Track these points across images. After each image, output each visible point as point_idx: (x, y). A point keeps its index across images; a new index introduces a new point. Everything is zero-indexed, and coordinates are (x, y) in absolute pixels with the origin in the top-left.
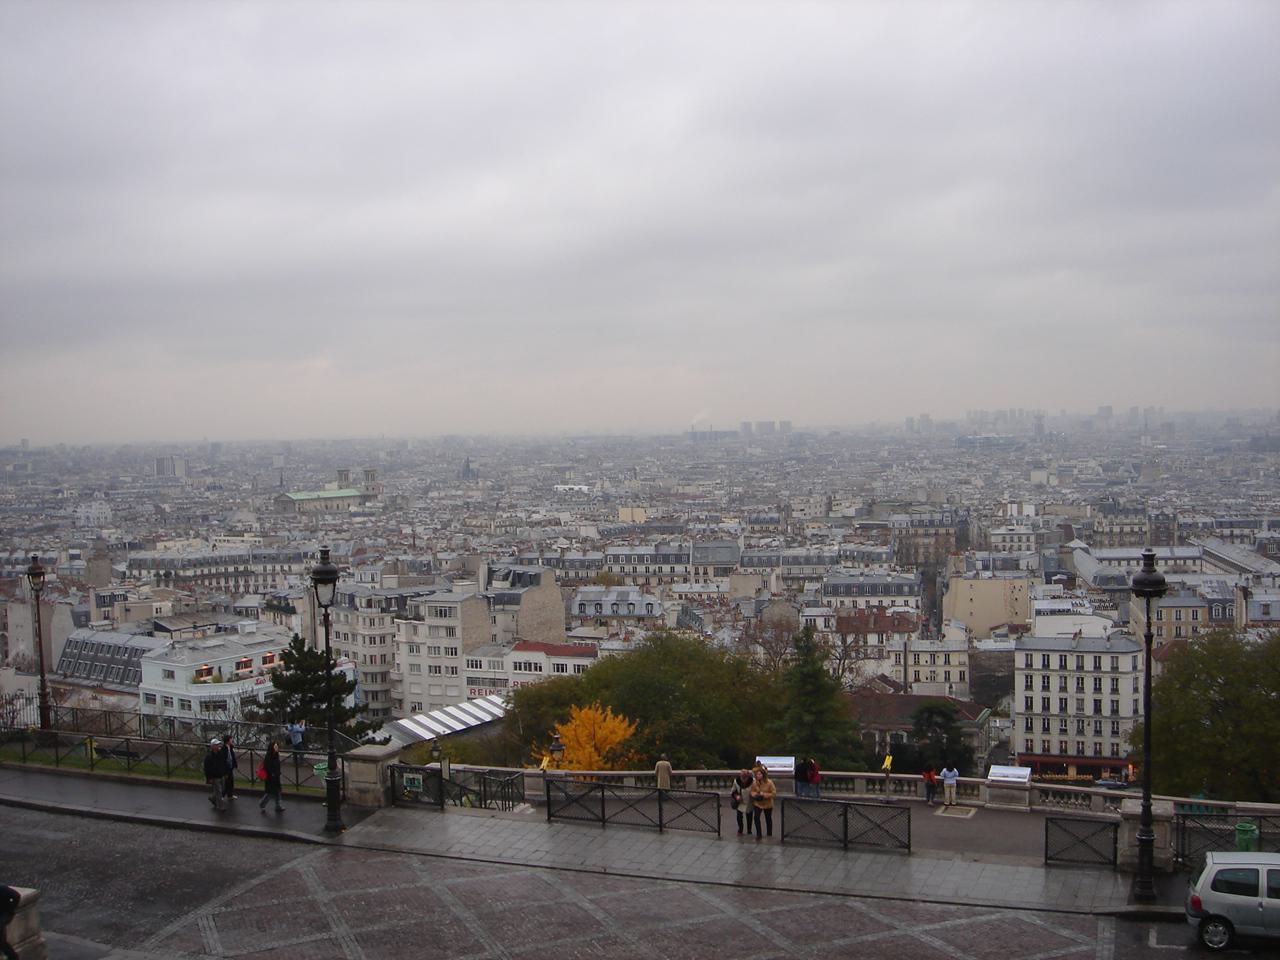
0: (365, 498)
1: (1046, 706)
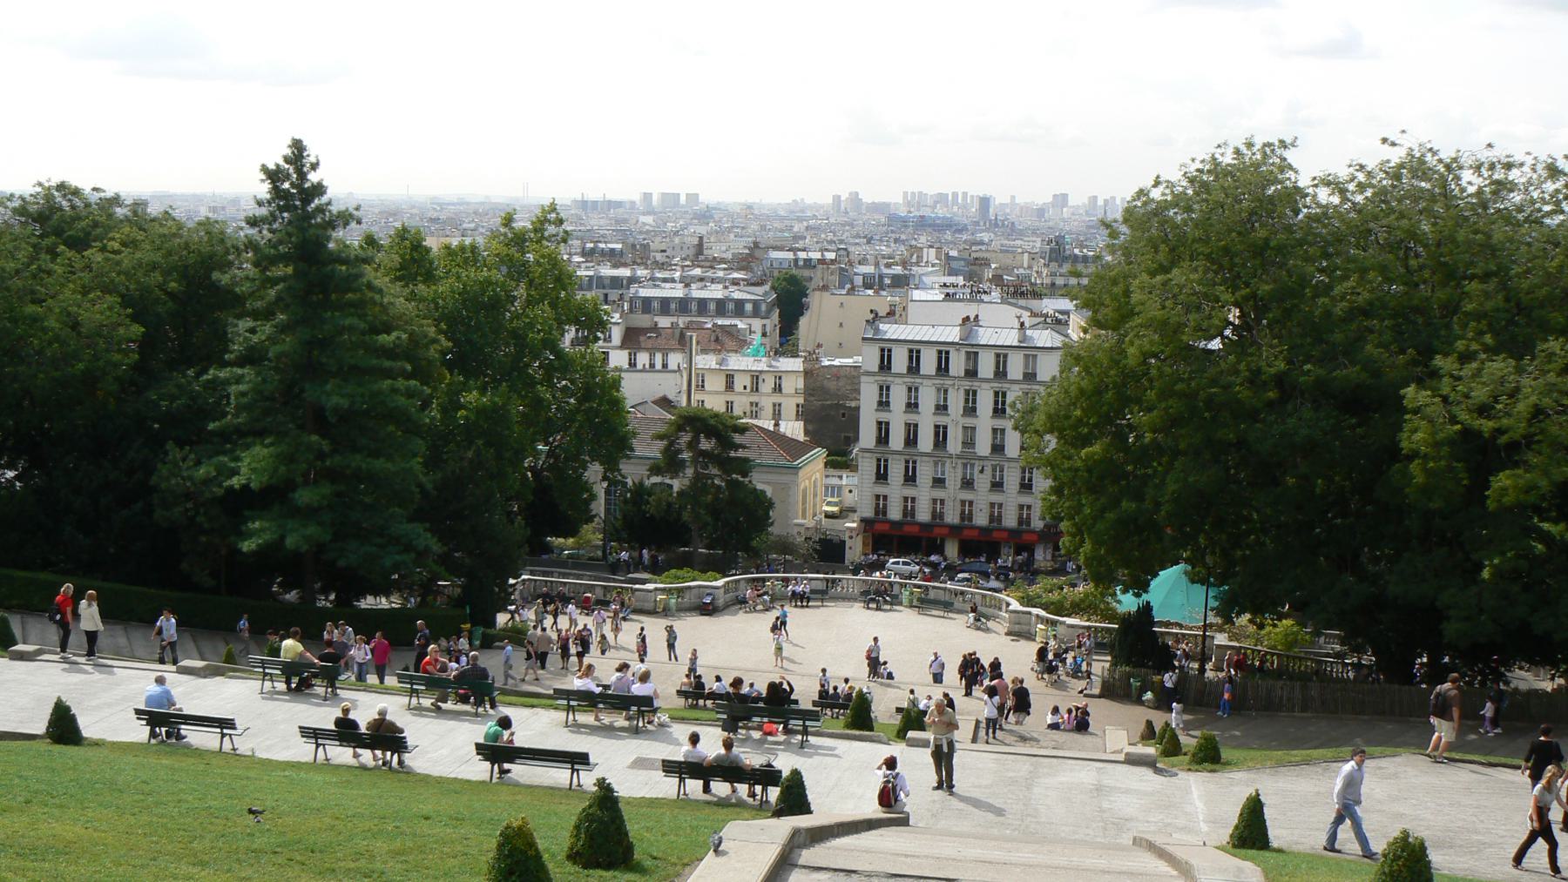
1: (911, 439)
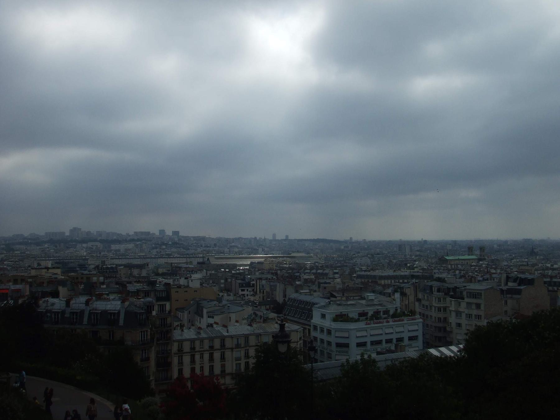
0: (480, 260)
